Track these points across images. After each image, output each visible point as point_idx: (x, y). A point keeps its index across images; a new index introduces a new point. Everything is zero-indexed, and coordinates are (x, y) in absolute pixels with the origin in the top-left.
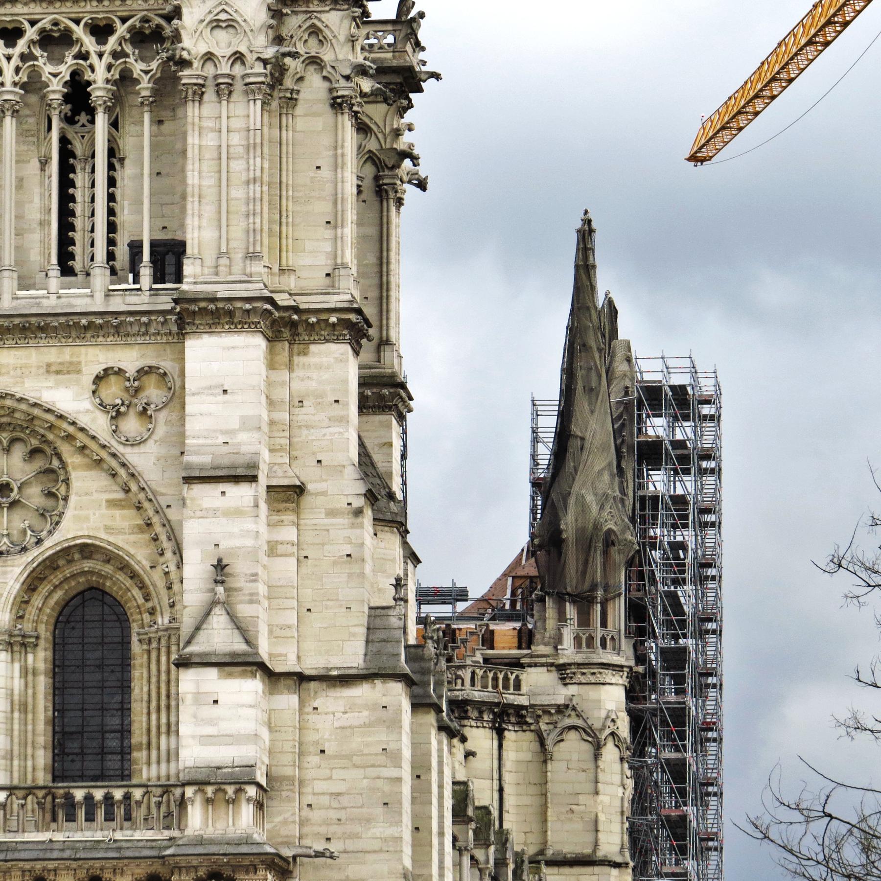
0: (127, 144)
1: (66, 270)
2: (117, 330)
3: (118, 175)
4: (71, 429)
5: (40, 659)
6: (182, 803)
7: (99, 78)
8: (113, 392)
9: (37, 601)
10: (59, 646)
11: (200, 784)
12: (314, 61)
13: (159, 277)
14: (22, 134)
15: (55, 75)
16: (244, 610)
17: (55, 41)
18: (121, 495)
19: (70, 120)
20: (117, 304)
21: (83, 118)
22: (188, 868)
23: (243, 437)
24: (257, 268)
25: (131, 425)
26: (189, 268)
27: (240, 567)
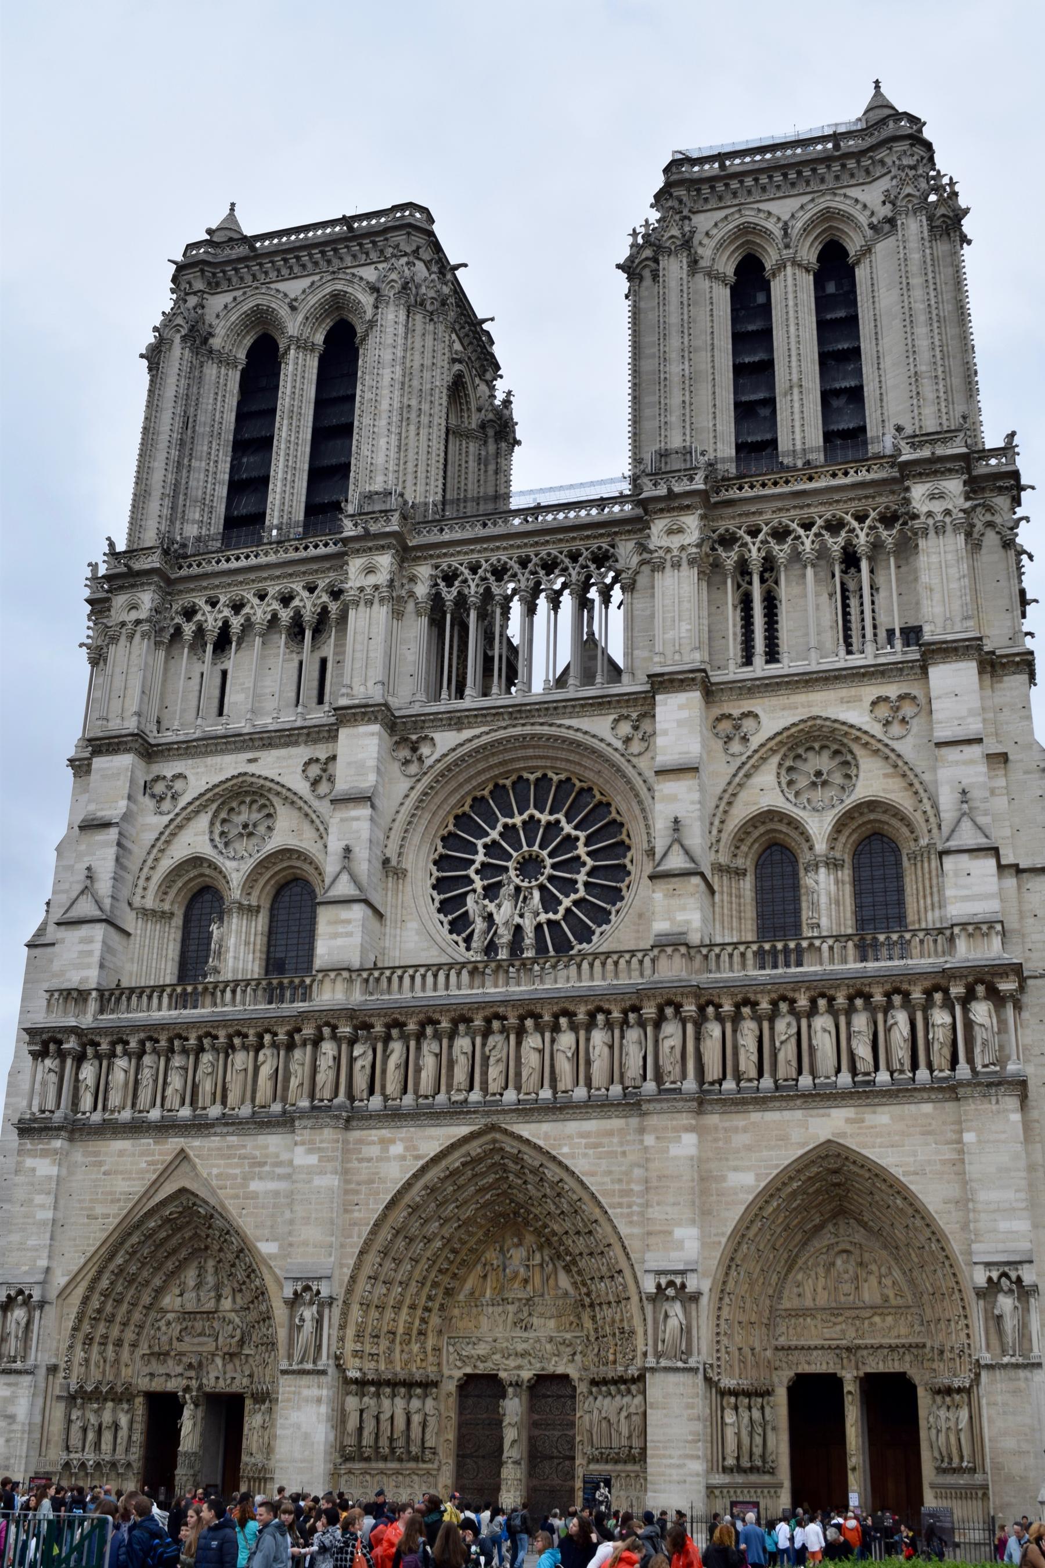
0: (881, 580)
1: (849, 652)
2: (883, 673)
3: (876, 599)
4: (858, 734)
5: (846, 874)
6: (952, 939)
7: (862, 539)
8: (883, 711)
9: (842, 839)
10: (856, 869)
11: (964, 925)
12: (990, 524)
13: (907, 644)
14: (817, 581)
15: (835, 544)
16: (982, 820)
17: (834, 526)
18: (891, 770)
19: (844, 572)
20: (882, 660)
21: (853, 570)
22: (961, 977)
23: (970, 720)
24: (970, 623)
25: (896, 729)
26: (926, 628)
27: (975, 794)
